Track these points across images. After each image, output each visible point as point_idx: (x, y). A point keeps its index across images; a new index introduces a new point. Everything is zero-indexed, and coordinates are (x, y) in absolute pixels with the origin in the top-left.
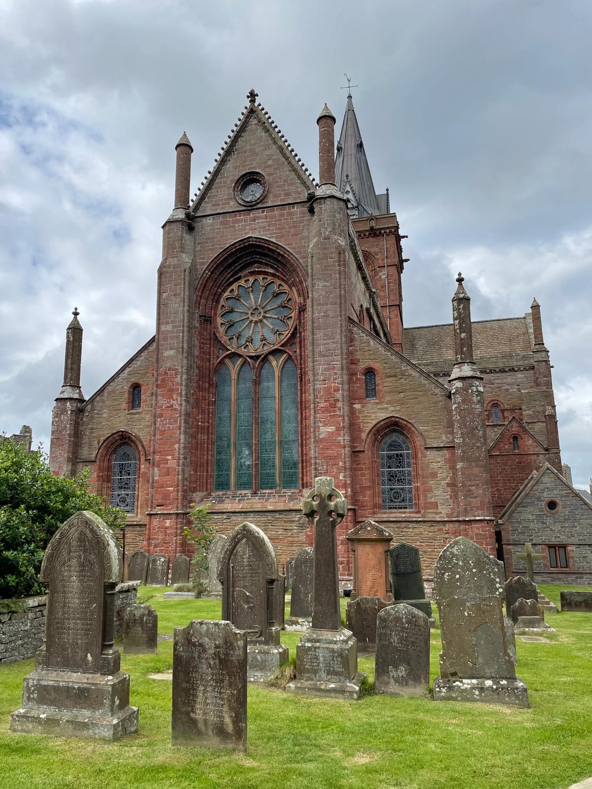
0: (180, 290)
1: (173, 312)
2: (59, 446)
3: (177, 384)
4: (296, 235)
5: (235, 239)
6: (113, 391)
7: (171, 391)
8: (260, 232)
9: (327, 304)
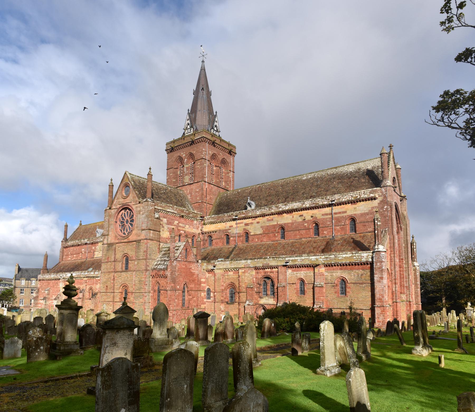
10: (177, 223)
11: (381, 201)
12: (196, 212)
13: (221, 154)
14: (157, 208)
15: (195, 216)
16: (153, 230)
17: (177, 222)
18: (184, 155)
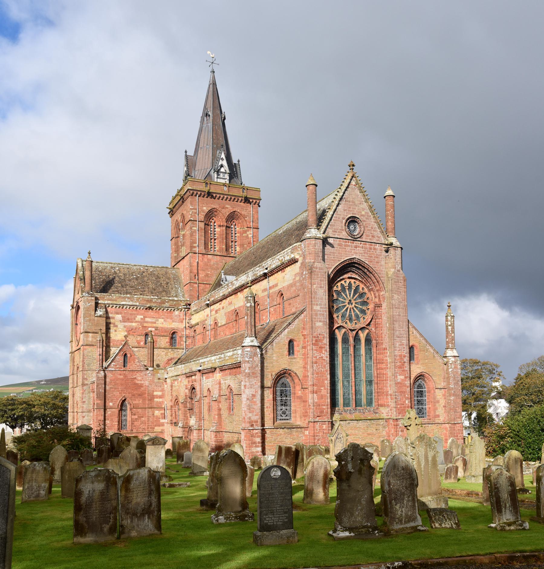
0: (323, 285)
1: (320, 298)
2: (254, 377)
3: (324, 344)
4: (378, 262)
5: (346, 257)
6: (279, 343)
7: (321, 348)
8: (360, 256)
9: (399, 308)
10: (141, 319)
11: (302, 264)
12: (176, 299)
13: (227, 206)
14: (103, 302)
15: (175, 305)
16: (93, 333)
17: (142, 317)
18: (180, 219)
